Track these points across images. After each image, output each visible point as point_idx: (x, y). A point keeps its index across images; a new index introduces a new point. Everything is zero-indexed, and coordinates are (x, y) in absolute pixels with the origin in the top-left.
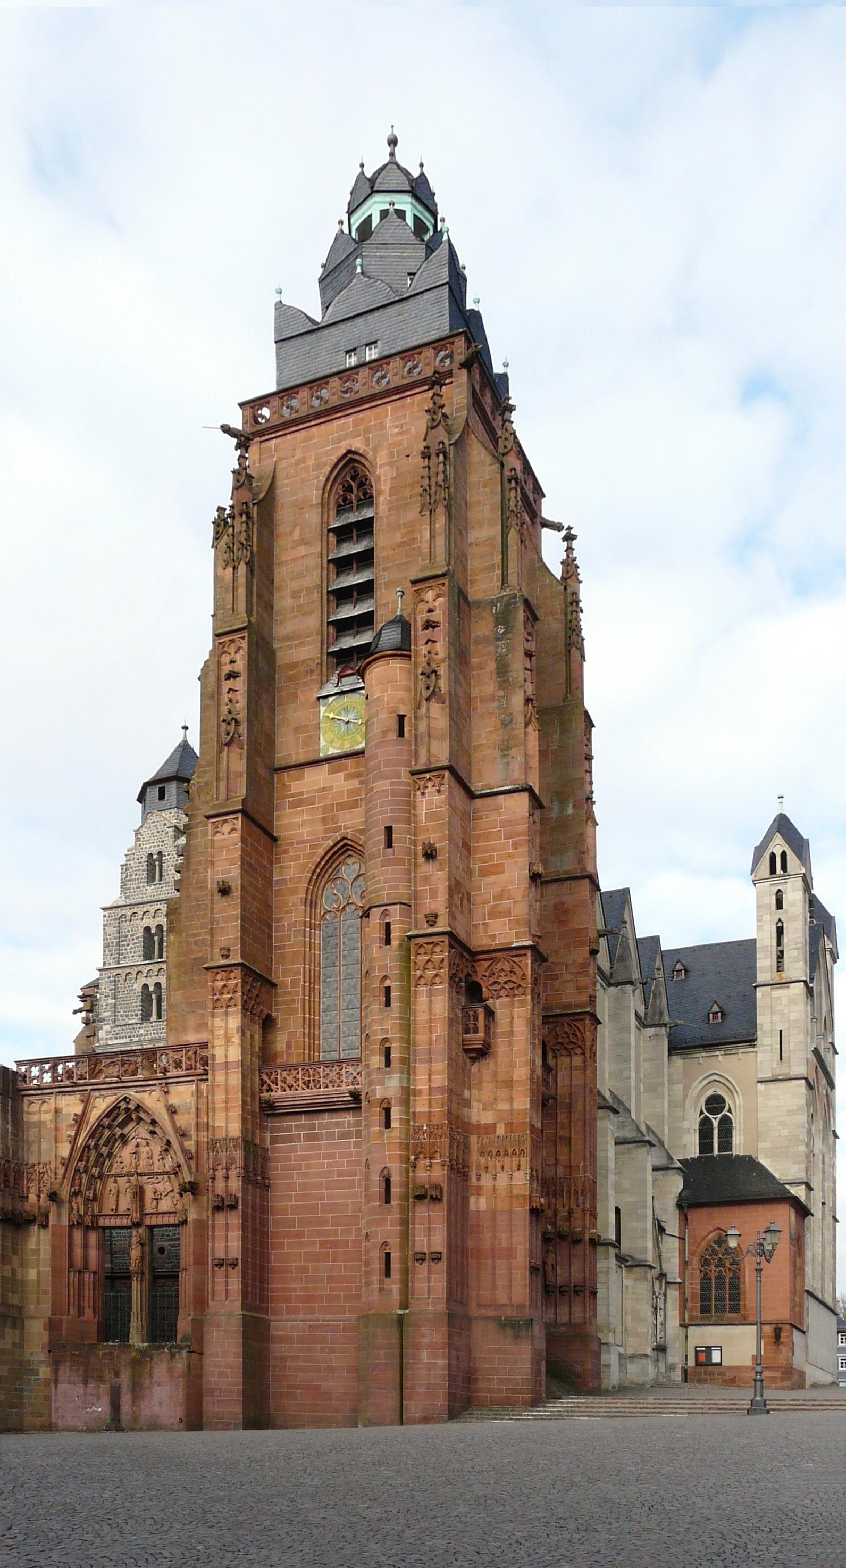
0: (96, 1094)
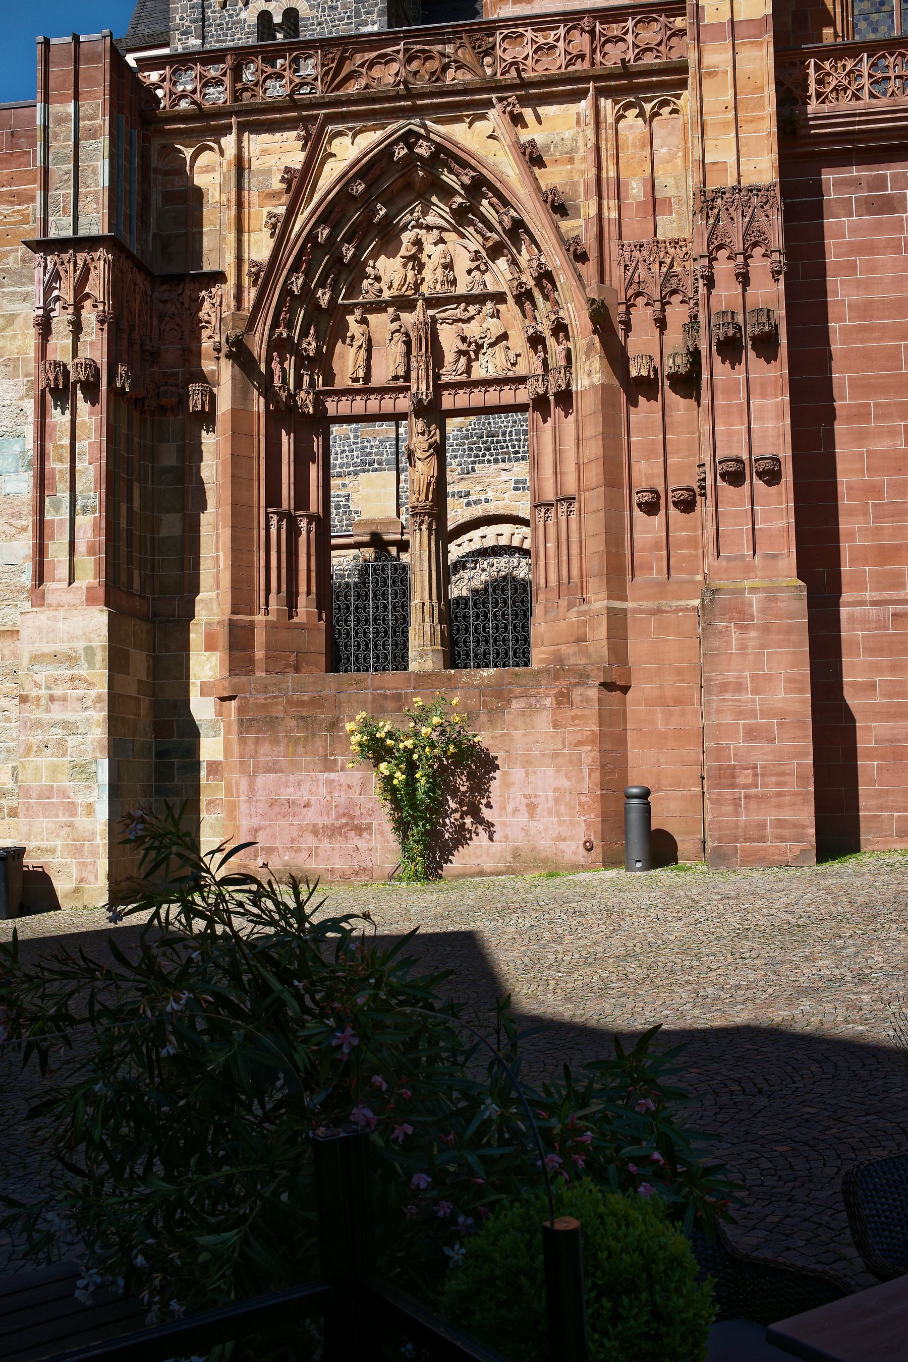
0: (339, 127)
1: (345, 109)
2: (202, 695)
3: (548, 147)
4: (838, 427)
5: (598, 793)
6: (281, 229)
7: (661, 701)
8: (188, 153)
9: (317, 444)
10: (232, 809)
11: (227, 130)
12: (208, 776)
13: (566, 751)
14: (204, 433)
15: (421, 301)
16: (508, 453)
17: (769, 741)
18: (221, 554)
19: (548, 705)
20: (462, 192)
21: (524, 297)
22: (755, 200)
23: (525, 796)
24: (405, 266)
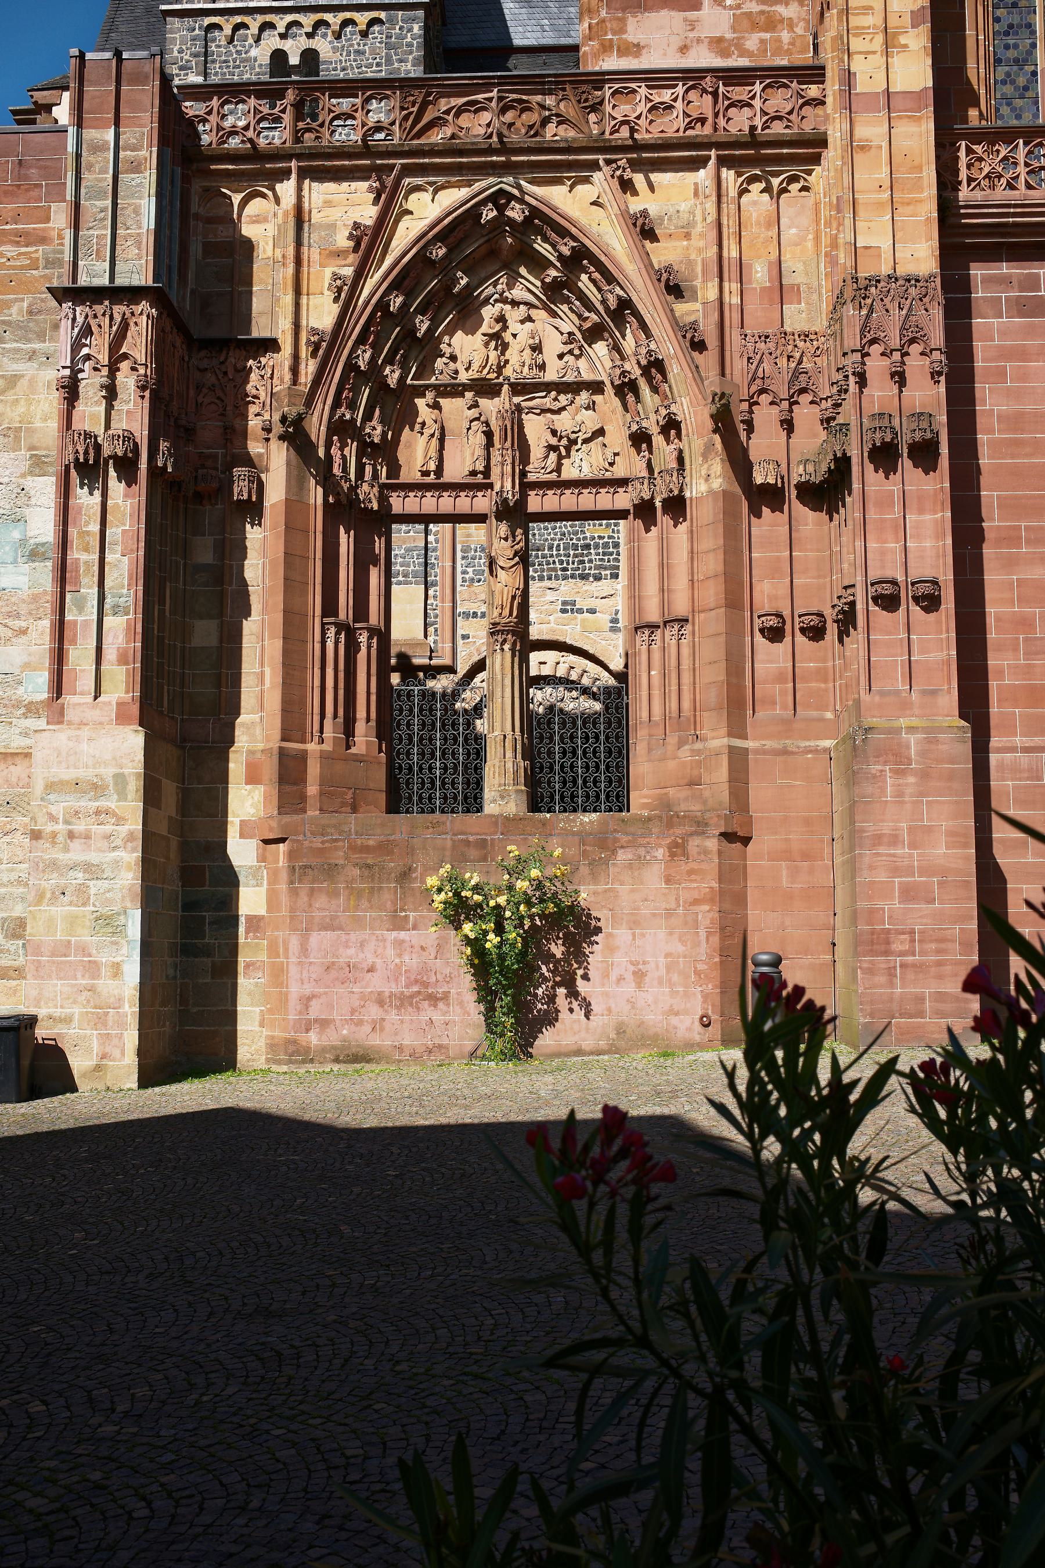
0: (419, 181)
1: (427, 160)
2: (242, 836)
3: (661, 218)
4: (987, 551)
5: (717, 959)
6: (347, 294)
7: (786, 855)
8: (237, 199)
9: (379, 545)
10: (278, 975)
11: (285, 174)
12: (247, 933)
13: (680, 910)
14: (248, 526)
15: (506, 388)
16: (555, 570)
17: (929, 903)
18: (267, 671)
19: (660, 857)
20: (558, 264)
21: (626, 389)
22: (913, 291)
23: (632, 963)
24: (486, 345)
